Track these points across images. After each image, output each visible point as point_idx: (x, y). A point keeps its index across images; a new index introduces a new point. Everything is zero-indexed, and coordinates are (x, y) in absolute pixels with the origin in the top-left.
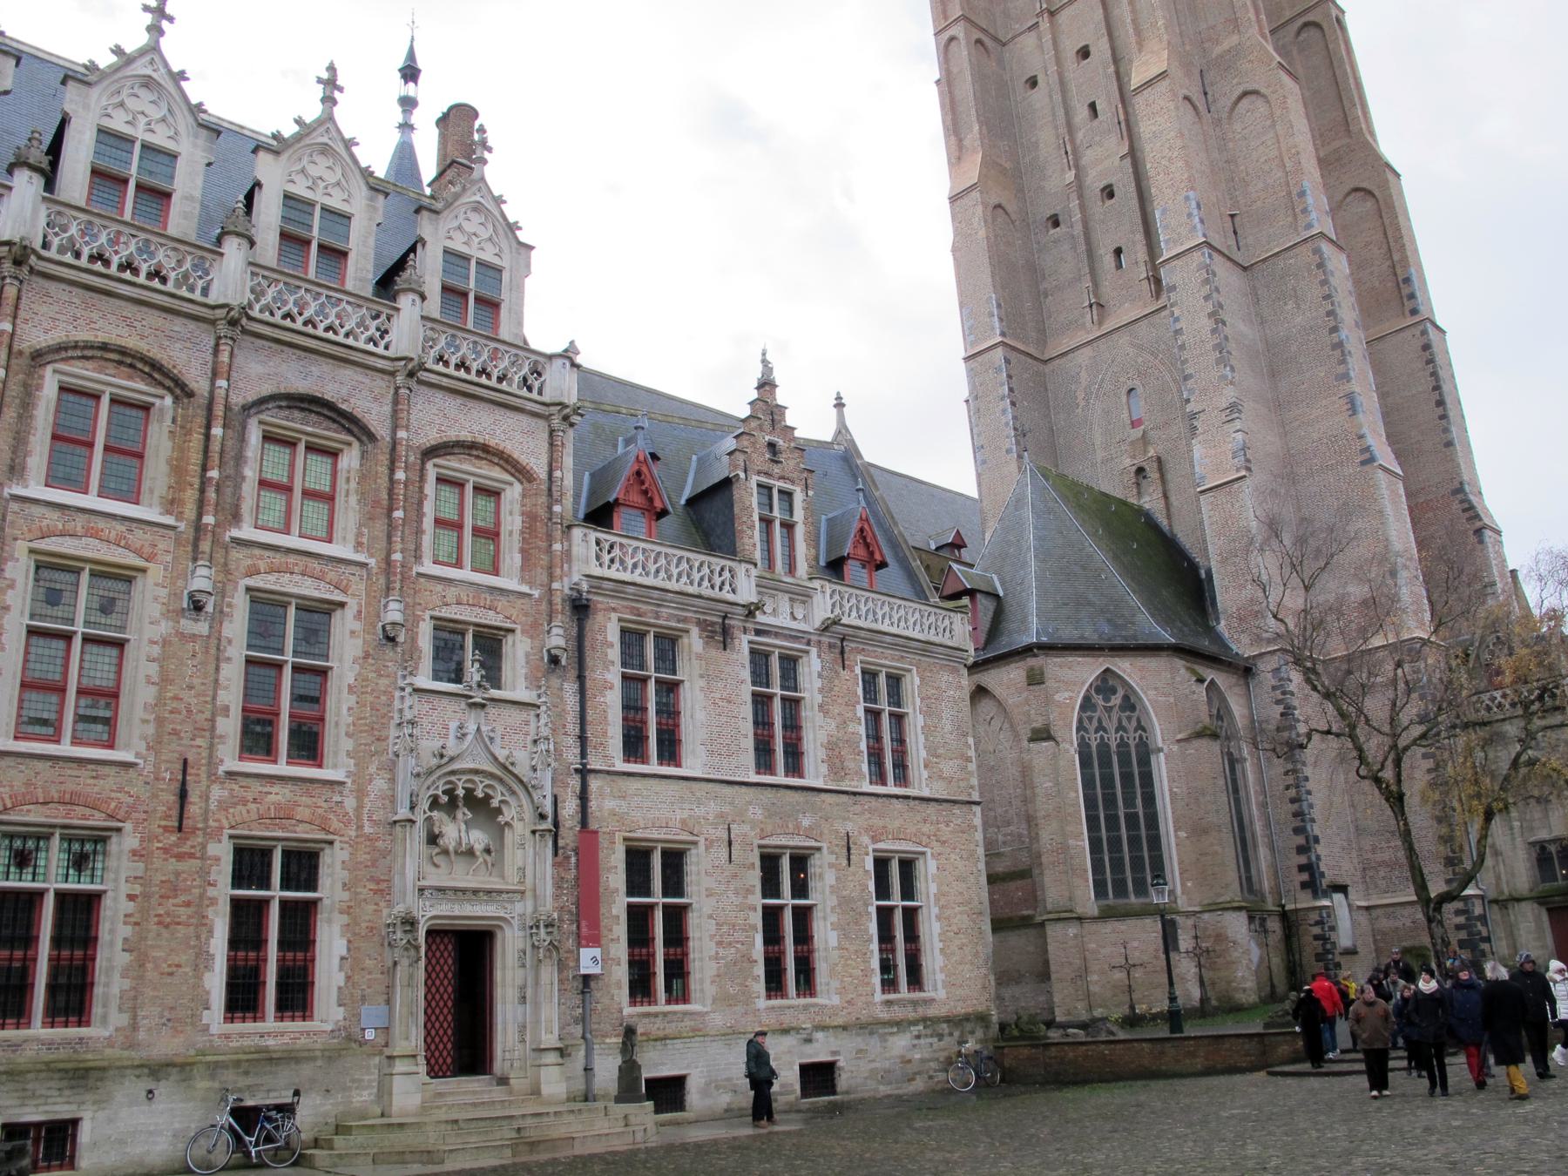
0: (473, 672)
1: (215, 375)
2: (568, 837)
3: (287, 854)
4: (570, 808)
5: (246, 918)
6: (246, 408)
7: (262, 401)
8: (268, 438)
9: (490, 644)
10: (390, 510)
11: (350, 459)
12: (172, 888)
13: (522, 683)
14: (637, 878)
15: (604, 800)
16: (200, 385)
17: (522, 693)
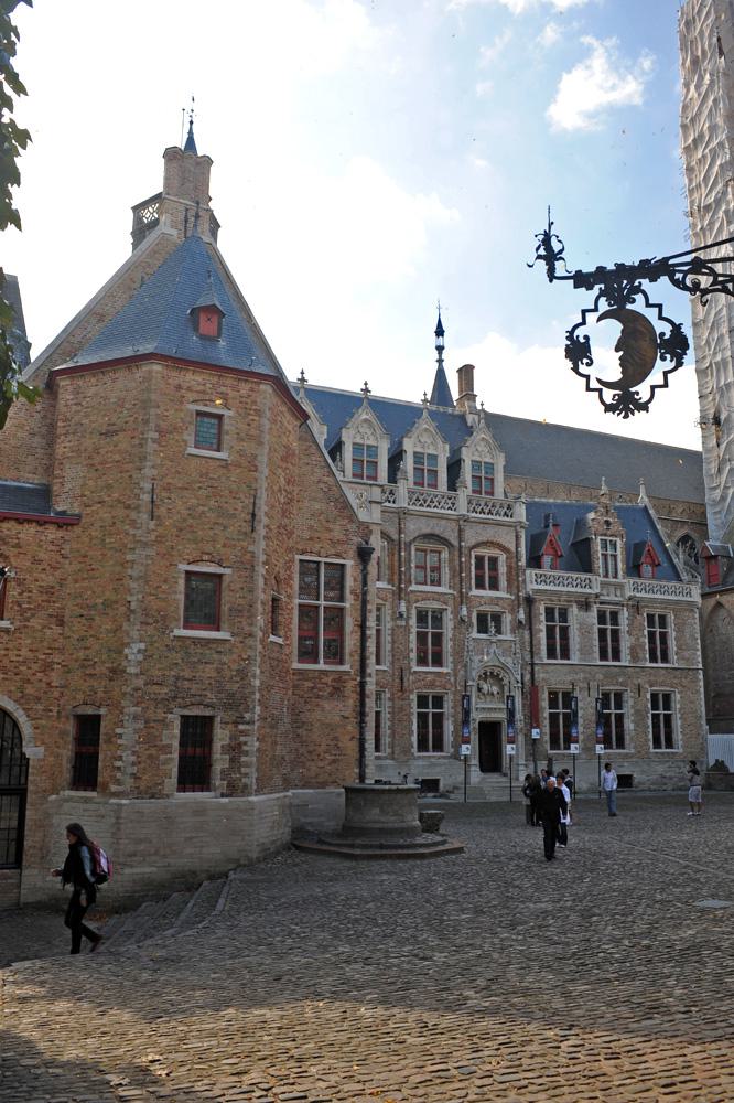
0: (493, 630)
1: (400, 532)
2: (527, 689)
3: (433, 697)
4: (527, 677)
5: (422, 718)
6: (410, 543)
7: (415, 539)
8: (417, 550)
9: (497, 618)
10: (461, 572)
11: (445, 555)
12: (401, 709)
13: (509, 631)
14: (553, 703)
15: (540, 675)
16: (395, 537)
17: (509, 637)
